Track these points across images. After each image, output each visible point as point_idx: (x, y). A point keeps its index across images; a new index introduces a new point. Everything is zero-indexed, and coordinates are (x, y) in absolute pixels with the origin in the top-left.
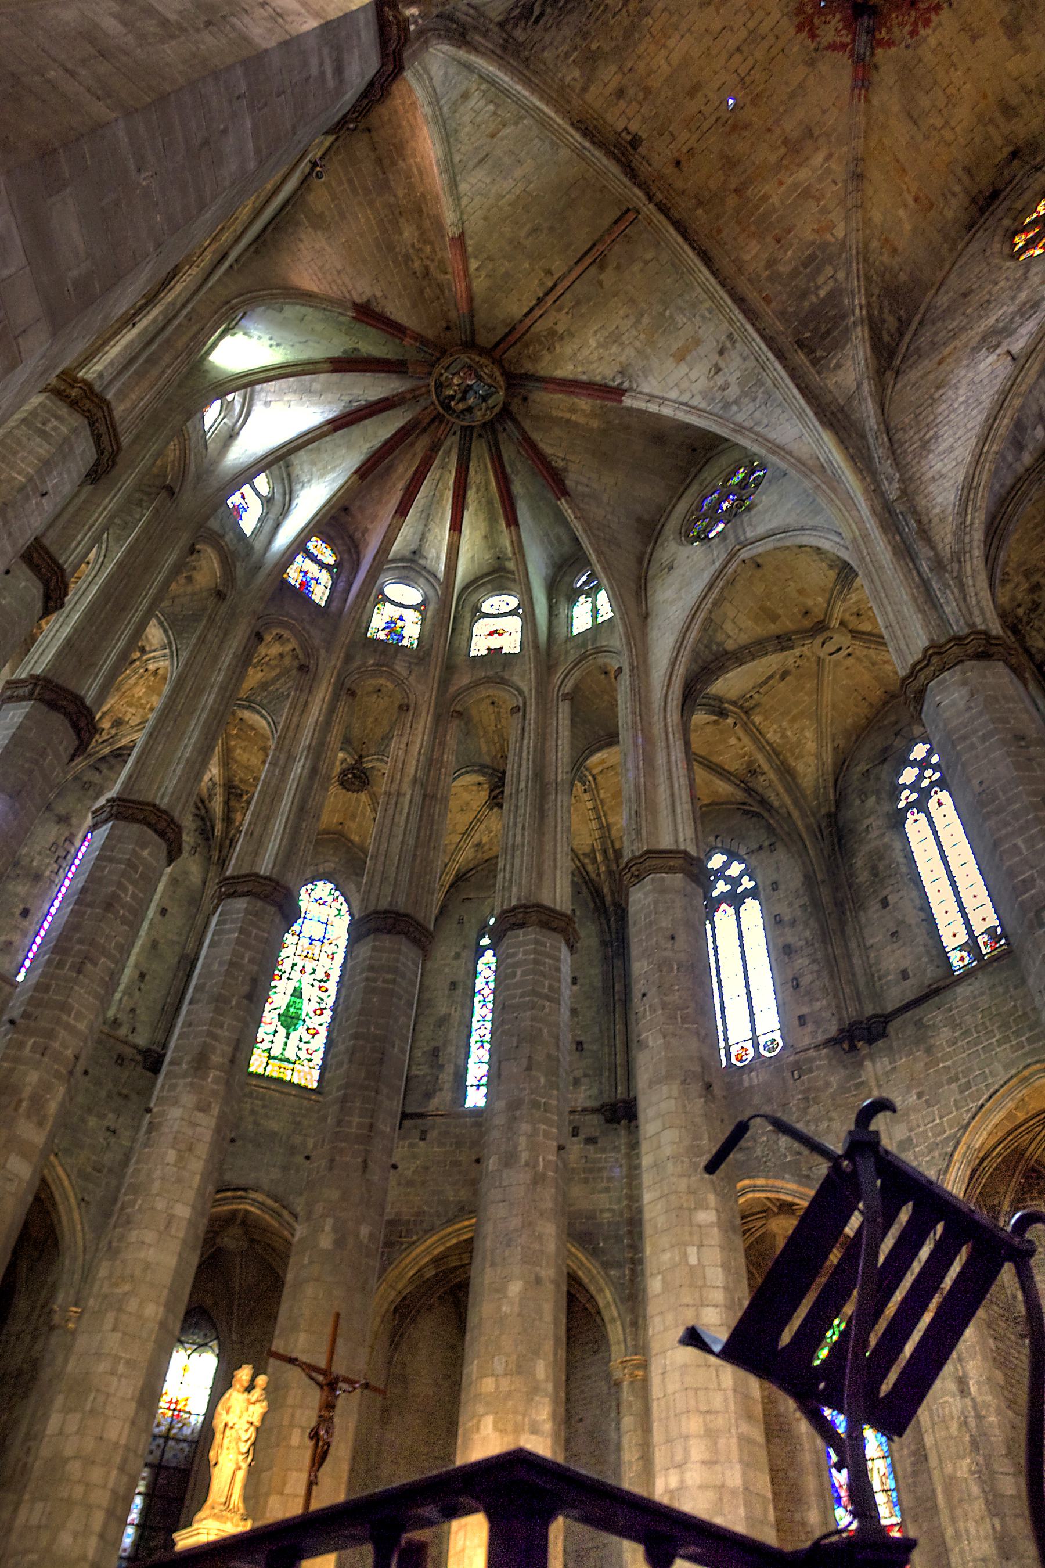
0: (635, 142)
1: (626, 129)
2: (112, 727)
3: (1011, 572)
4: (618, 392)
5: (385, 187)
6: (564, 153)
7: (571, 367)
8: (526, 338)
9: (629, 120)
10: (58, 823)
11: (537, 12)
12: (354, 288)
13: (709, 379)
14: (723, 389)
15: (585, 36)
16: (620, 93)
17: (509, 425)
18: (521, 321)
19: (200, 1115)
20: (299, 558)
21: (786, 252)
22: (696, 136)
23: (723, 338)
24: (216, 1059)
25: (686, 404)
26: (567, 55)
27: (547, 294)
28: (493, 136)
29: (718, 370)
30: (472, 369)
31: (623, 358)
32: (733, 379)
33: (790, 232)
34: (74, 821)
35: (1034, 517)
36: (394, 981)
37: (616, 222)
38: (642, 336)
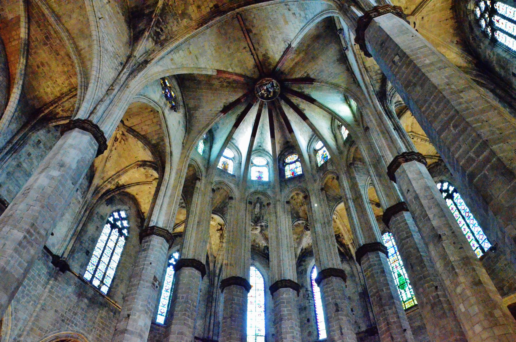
0: (216, 6)
1: (211, 8)
5: (199, 82)
6: (208, 31)
11: (159, 30)
13: (296, 18)
14: (300, 16)
15: (176, 14)
16: (199, 7)
18: (256, 63)
20: (287, 168)
25: (301, 29)
27: (251, 51)
29: (294, 14)
30: (261, 86)
31: (281, 39)
32: (299, 11)
34: (304, 284)
36: (372, 270)
37: (239, 21)
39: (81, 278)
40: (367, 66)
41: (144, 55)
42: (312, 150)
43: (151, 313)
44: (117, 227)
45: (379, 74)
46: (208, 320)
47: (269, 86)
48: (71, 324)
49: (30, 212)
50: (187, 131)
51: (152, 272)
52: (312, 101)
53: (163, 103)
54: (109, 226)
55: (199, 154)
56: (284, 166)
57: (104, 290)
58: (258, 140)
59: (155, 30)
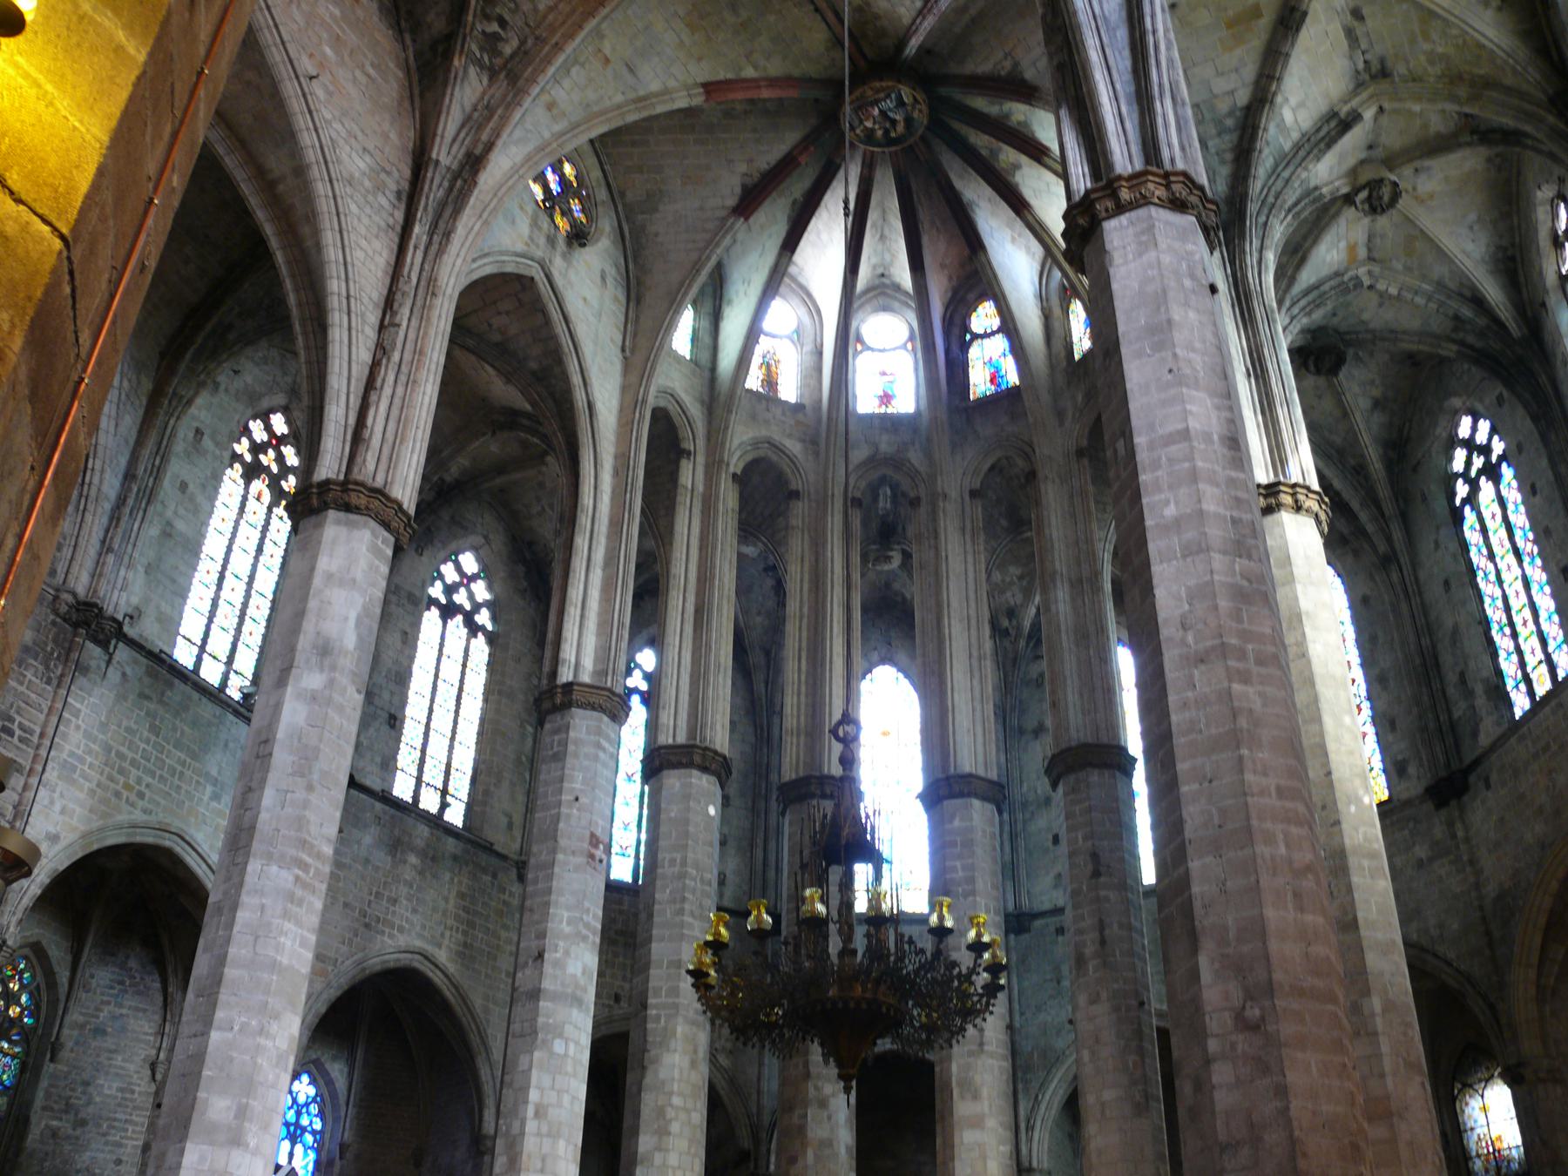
2: (1010, 620)
10: (1037, 737)
11: (494, 27)
17: (944, 91)
20: (975, 353)
24: (1089, 950)
39: (387, 799)
41: (462, 135)
43: (594, 934)
44: (458, 609)
45: (1230, 131)
46: (759, 853)
47: (889, 104)
48: (387, 930)
49: (288, 810)
50: (633, 295)
51: (583, 822)
53: (542, 241)
54: (431, 618)
55: (678, 358)
56: (965, 347)
57: (455, 816)
58: (874, 260)
59: (484, 32)
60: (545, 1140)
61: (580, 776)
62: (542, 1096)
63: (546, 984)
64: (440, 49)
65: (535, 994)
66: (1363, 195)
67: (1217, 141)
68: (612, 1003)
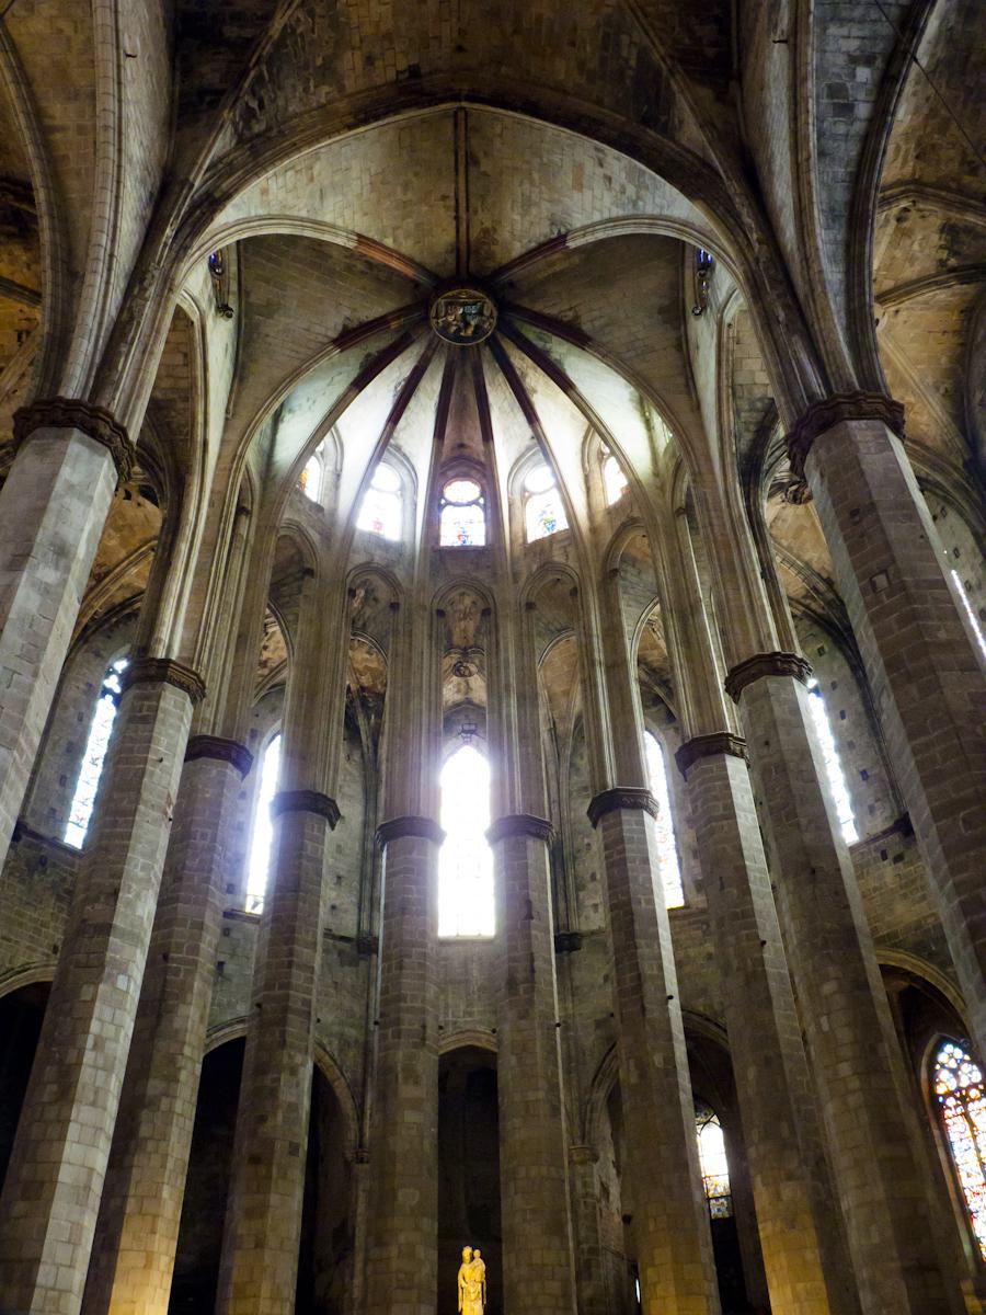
0: (414, 72)
3: (975, 158)
4: (561, 239)
7: (518, 245)
8: (473, 248)
9: (395, 65)
11: (254, 104)
12: (327, 329)
13: (610, 189)
14: (623, 191)
16: (370, 60)
19: (522, 1022)
21: (585, 48)
22: (454, 20)
23: (594, 153)
25: (610, 220)
26: (306, 90)
28: (312, 179)
29: (609, 179)
31: (545, 214)
33: (575, 29)
35: (957, 97)
37: (456, 125)
38: (543, 188)
40: (740, 380)
42: (517, 486)
45: (758, 411)
49: (13, 690)
50: (238, 373)
52: (566, 385)
56: (441, 507)
59: (247, 104)
60: (100, 1072)
61: (164, 740)
62: (102, 1029)
63: (118, 922)
64: (208, 99)
65: (106, 929)
66: (794, 487)
67: (748, 414)
68: (50, 952)
